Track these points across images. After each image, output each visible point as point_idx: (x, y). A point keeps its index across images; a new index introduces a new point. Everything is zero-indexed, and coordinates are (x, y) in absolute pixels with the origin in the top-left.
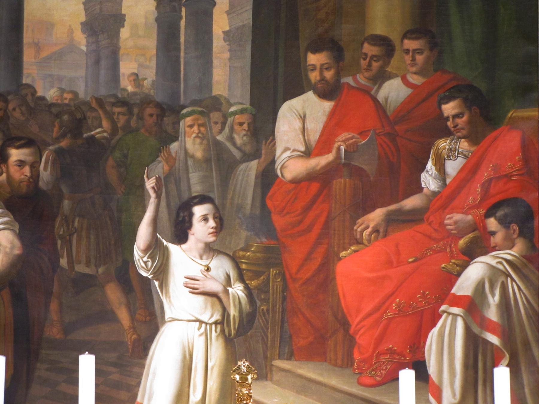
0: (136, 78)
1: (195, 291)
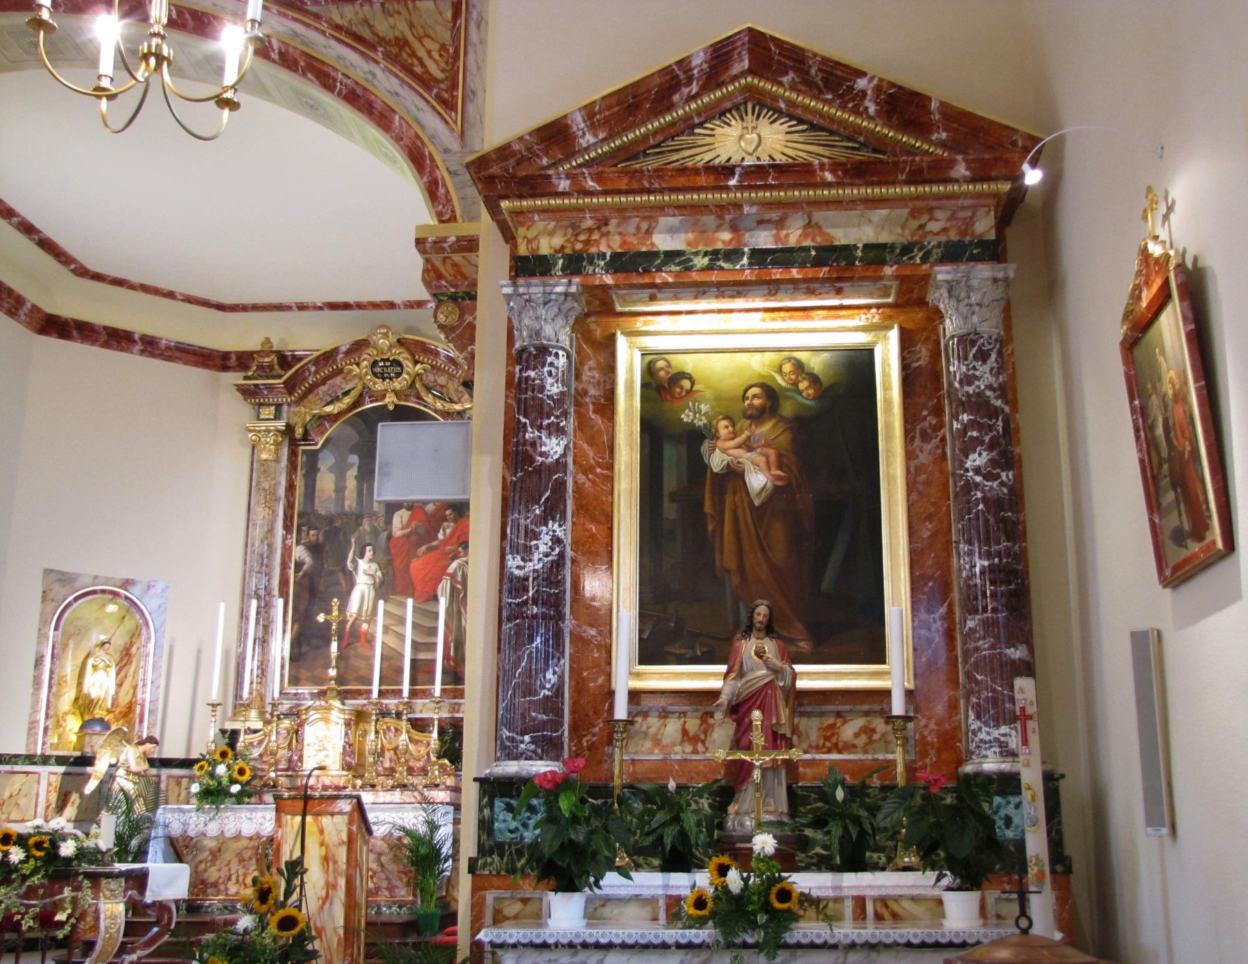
0: (350, 507)
1: (366, 574)
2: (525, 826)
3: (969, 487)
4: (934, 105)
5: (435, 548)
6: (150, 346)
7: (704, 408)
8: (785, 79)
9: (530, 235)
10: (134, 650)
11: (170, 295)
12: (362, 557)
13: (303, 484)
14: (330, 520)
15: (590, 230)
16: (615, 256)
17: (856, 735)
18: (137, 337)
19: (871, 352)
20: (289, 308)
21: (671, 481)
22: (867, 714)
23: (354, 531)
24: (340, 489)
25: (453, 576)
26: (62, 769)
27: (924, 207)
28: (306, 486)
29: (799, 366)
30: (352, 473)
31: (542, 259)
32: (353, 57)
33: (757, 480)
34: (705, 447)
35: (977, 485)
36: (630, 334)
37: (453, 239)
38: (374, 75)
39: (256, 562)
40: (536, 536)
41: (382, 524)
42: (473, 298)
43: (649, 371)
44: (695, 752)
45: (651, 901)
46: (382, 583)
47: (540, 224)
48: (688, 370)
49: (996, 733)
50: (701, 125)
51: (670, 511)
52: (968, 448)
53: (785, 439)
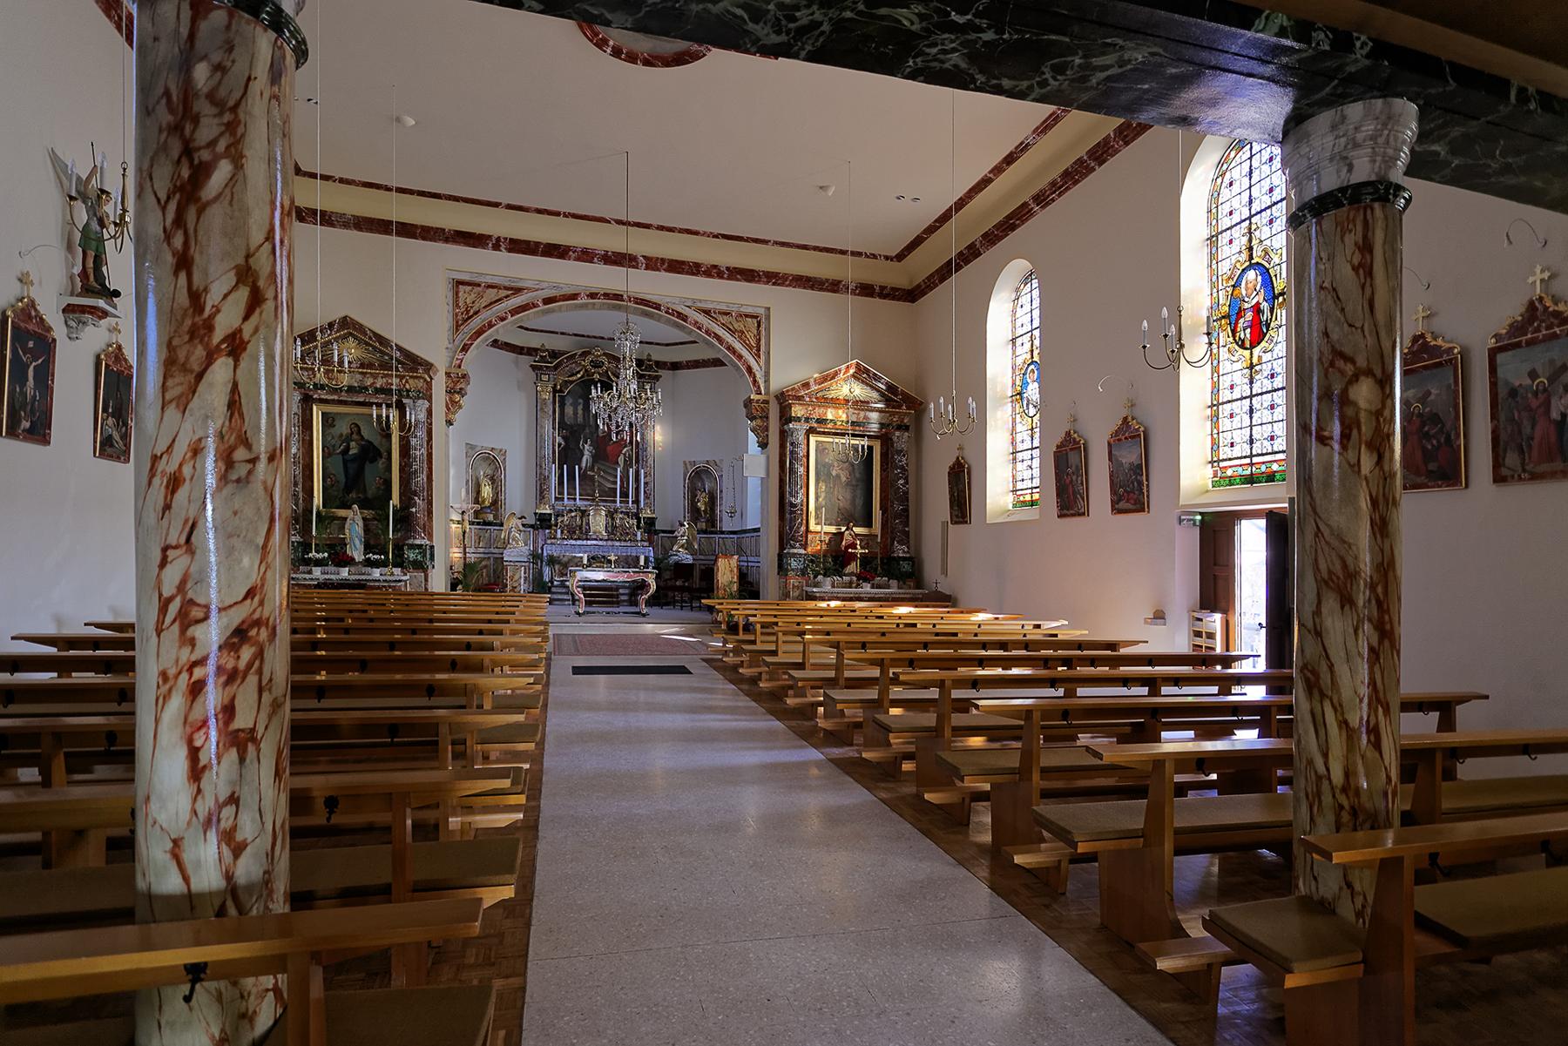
20: (557, 333)
24: (575, 413)
25: (625, 454)
30: (580, 407)
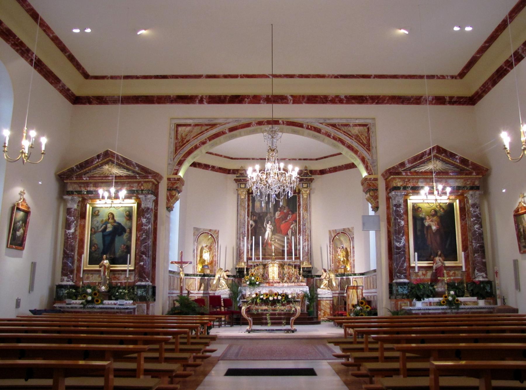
1: (269, 228)
2: (404, 290)
3: (475, 231)
4: (470, 162)
5: (287, 221)
6: (213, 168)
7: (424, 214)
8: (443, 155)
9: (396, 182)
10: (212, 247)
11: (221, 156)
12: (268, 223)
13: (251, 204)
14: (259, 214)
15: (407, 182)
16: (412, 187)
17: (453, 274)
18: (210, 166)
19: (453, 204)
20: (250, 159)
21: (418, 228)
22: (454, 270)
23: (266, 217)
25: (292, 229)
26: (200, 277)
27: (466, 180)
28: (252, 205)
29: (440, 206)
31: (399, 187)
32: (348, 138)
33: (434, 228)
34: (424, 221)
35: (477, 231)
36: (410, 199)
37: (373, 178)
38: (352, 143)
39: (240, 225)
40: (402, 239)
41: (273, 215)
42: (377, 190)
43: (413, 206)
44: (425, 277)
45: (427, 303)
46: (273, 230)
47: (398, 180)
48: (420, 206)
49: (481, 274)
50: (426, 162)
51: (419, 233)
52: (475, 224)
53: (438, 220)
